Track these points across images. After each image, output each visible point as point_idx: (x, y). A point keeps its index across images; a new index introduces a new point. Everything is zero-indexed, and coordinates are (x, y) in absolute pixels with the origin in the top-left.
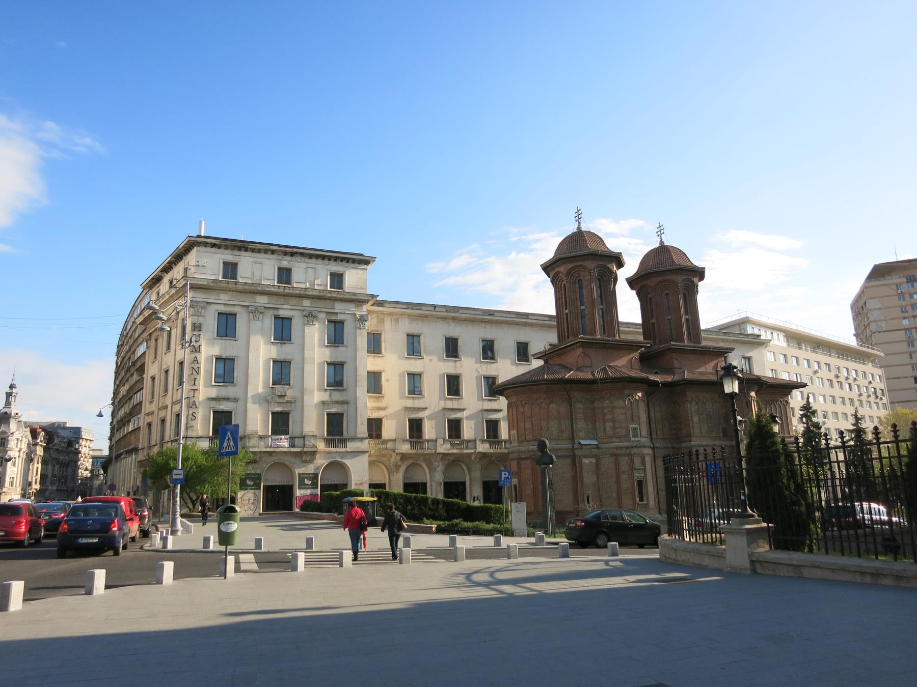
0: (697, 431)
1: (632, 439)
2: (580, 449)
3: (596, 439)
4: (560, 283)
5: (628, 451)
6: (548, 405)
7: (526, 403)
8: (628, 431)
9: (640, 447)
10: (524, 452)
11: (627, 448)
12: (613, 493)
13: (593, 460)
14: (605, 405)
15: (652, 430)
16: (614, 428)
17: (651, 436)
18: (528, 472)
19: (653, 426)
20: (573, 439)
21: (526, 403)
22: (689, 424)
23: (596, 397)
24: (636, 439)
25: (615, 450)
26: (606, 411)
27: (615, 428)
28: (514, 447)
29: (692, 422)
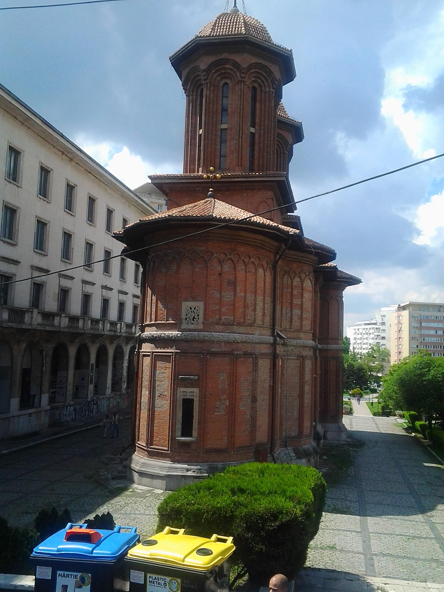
4: (219, 78)
7: (228, 259)
10: (219, 342)
12: (295, 413)
14: (295, 283)
18: (223, 377)
20: (273, 329)
21: (228, 259)
25: (301, 349)
28: (195, 330)
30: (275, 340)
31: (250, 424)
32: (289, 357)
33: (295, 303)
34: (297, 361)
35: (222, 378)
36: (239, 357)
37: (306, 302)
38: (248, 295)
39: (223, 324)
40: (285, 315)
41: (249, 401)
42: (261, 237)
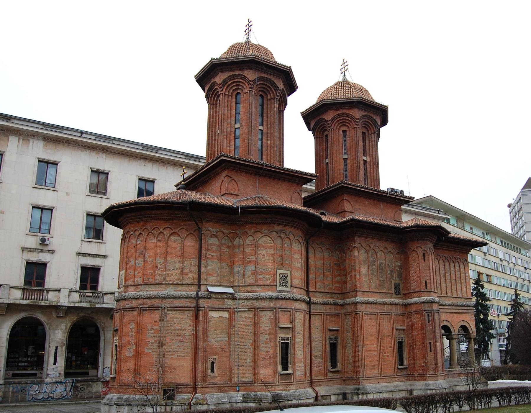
0: (364, 285)
1: (279, 288)
2: (207, 298)
3: (232, 287)
5: (272, 305)
6: (169, 237)
8: (274, 278)
9: (289, 299)
10: (131, 299)
11: (271, 299)
13: (226, 315)
15: (310, 280)
16: (256, 273)
17: (308, 287)
18: (133, 326)
19: (311, 276)
20: (199, 285)
22: (355, 276)
23: (238, 232)
24: (285, 289)
25: (255, 302)
26: (248, 250)
27: (258, 273)
29: (360, 273)
30: (197, 294)
31: (156, 365)
32: (239, 310)
33: (249, 260)
34: (249, 313)
35: (131, 327)
36: (143, 310)
37: (264, 258)
38: (158, 259)
39: (135, 286)
40: (237, 272)
41: (156, 345)
42: (167, 211)
